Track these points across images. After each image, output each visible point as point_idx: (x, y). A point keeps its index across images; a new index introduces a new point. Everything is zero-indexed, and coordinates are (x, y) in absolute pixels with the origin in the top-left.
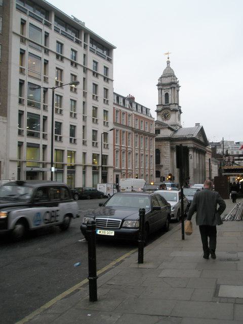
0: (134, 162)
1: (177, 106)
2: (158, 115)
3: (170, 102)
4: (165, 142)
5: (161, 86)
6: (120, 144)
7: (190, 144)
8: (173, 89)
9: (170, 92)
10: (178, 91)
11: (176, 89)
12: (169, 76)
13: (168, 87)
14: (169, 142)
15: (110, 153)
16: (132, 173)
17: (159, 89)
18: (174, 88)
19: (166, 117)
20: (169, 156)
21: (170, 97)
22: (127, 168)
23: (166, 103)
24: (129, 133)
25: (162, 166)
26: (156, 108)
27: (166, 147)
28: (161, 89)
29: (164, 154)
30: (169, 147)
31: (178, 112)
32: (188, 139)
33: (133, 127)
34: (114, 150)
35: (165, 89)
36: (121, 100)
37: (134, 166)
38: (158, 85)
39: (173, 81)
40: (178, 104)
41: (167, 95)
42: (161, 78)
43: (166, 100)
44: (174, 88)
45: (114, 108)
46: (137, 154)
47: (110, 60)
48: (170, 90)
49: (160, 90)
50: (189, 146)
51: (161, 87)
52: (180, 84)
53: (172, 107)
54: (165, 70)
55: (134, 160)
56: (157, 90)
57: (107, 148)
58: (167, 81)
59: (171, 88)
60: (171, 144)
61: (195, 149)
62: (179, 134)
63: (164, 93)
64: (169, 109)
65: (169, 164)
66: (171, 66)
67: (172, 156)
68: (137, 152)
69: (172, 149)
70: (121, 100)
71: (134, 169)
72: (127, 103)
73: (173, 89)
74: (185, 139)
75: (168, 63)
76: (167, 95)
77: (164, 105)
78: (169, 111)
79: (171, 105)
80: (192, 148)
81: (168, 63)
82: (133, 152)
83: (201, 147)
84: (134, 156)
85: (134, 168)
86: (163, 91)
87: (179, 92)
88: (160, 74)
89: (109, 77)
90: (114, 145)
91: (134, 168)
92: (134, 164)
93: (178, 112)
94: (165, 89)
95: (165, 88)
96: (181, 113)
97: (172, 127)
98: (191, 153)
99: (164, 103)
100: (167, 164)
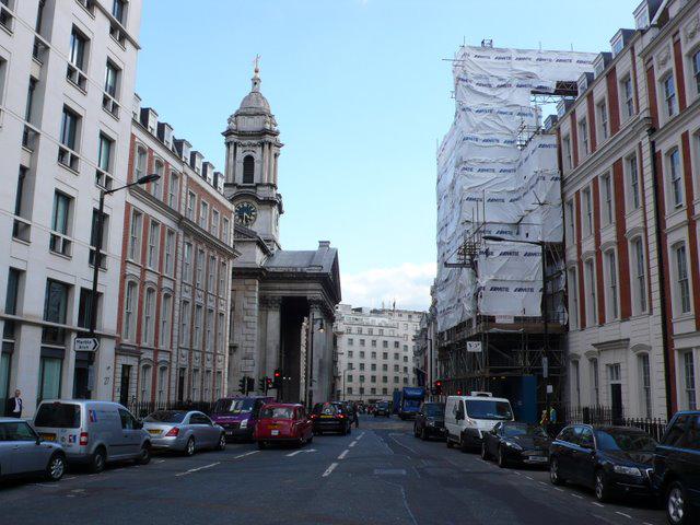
0: (176, 326)
3: (256, 180)
4: (248, 282)
5: (233, 136)
6: (144, 260)
8: (266, 147)
9: (257, 156)
10: (276, 156)
11: (274, 149)
12: (258, 114)
15: (109, 284)
16: (170, 363)
17: (228, 144)
20: (256, 320)
22: (156, 344)
24: (171, 233)
27: (249, 294)
30: (256, 295)
32: (309, 279)
33: (183, 213)
34: (124, 277)
37: (175, 339)
38: (227, 134)
39: (268, 126)
41: (249, 161)
45: (133, 136)
46: (186, 302)
49: (232, 148)
50: (310, 295)
51: (234, 138)
52: (281, 138)
53: (262, 193)
54: (248, 98)
55: (176, 320)
56: (225, 148)
59: (262, 145)
62: (278, 264)
63: (241, 156)
64: (256, 199)
65: (255, 345)
66: (263, 89)
67: (263, 323)
68: (187, 296)
69: (265, 303)
71: (175, 352)
73: (266, 147)
74: (301, 277)
75: (256, 82)
76: (249, 161)
77: (239, 187)
78: (254, 203)
79: (260, 189)
80: (318, 302)
81: (256, 82)
84: (177, 307)
85: (175, 347)
86: (239, 149)
87: (279, 158)
88: (235, 107)
90: (125, 262)
91: (175, 347)
92: (176, 333)
93: (275, 210)
95: (246, 142)
96: (281, 212)
99: (240, 181)
100: (250, 344)
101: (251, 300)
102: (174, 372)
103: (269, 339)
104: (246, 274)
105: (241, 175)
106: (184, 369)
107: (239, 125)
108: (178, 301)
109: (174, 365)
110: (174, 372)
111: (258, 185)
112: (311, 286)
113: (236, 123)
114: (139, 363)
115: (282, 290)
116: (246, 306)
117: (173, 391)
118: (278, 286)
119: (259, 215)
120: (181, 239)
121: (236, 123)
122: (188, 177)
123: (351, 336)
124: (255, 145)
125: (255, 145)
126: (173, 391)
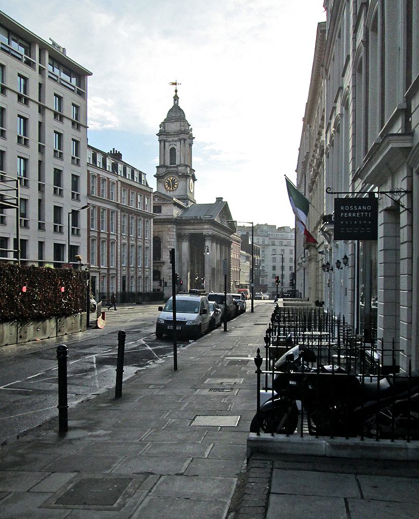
0: (119, 257)
1: (188, 169)
2: (158, 181)
3: (177, 163)
4: (169, 226)
5: (163, 134)
6: (99, 228)
7: (207, 230)
8: (182, 142)
9: (178, 147)
10: (191, 145)
11: (188, 141)
13: (176, 139)
14: (175, 226)
15: (81, 242)
16: (117, 275)
17: (160, 141)
18: (185, 140)
19: (172, 185)
21: (178, 153)
22: (108, 266)
23: (171, 164)
24: (113, 212)
25: (164, 263)
26: (155, 172)
27: (171, 233)
28: (165, 141)
29: (167, 244)
30: (175, 234)
31: (190, 177)
32: (204, 223)
34: (89, 237)
35: (169, 142)
36: (99, 158)
37: (119, 263)
40: (190, 167)
41: (173, 151)
42: (163, 123)
43: (171, 159)
44: (185, 140)
45: (88, 171)
47: (82, 94)
48: (178, 143)
49: (163, 143)
50: (205, 232)
51: (164, 137)
54: (171, 111)
55: (119, 253)
57: (78, 234)
58: (174, 127)
59: (180, 140)
60: (177, 229)
61: (214, 238)
64: (177, 173)
68: (125, 241)
69: (180, 237)
70: (99, 158)
71: (119, 269)
72: (109, 162)
73: (182, 142)
75: (176, 98)
77: (167, 167)
79: (180, 168)
80: (209, 236)
81: (176, 98)
82: (119, 241)
83: (223, 235)
84: (119, 247)
85: (119, 266)
87: (193, 146)
89: (81, 122)
90: (89, 231)
91: (119, 266)
92: (119, 260)
94: (169, 142)
96: (194, 180)
97: (181, 203)
98: (208, 243)
99: (168, 163)
101: (171, 236)
102: (119, 278)
103: (183, 257)
104: (168, 222)
105: (169, 161)
106: (125, 276)
107: (166, 129)
108: (119, 244)
109: (119, 275)
110: (119, 278)
111: (178, 166)
112: (206, 227)
113: (164, 128)
114: (100, 274)
115: (190, 230)
116: (169, 240)
117: (119, 287)
118: (188, 227)
119: (179, 186)
120: (119, 214)
121: (164, 128)
122: (121, 182)
123: (274, 247)
124: (176, 141)
125: (176, 141)
126: (119, 287)
